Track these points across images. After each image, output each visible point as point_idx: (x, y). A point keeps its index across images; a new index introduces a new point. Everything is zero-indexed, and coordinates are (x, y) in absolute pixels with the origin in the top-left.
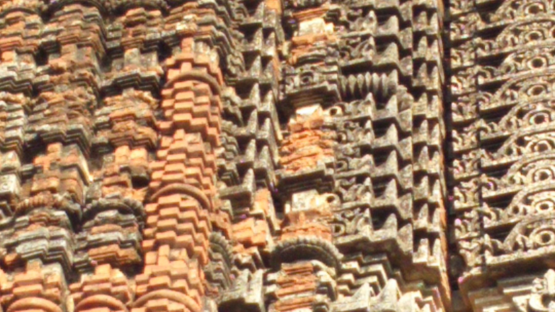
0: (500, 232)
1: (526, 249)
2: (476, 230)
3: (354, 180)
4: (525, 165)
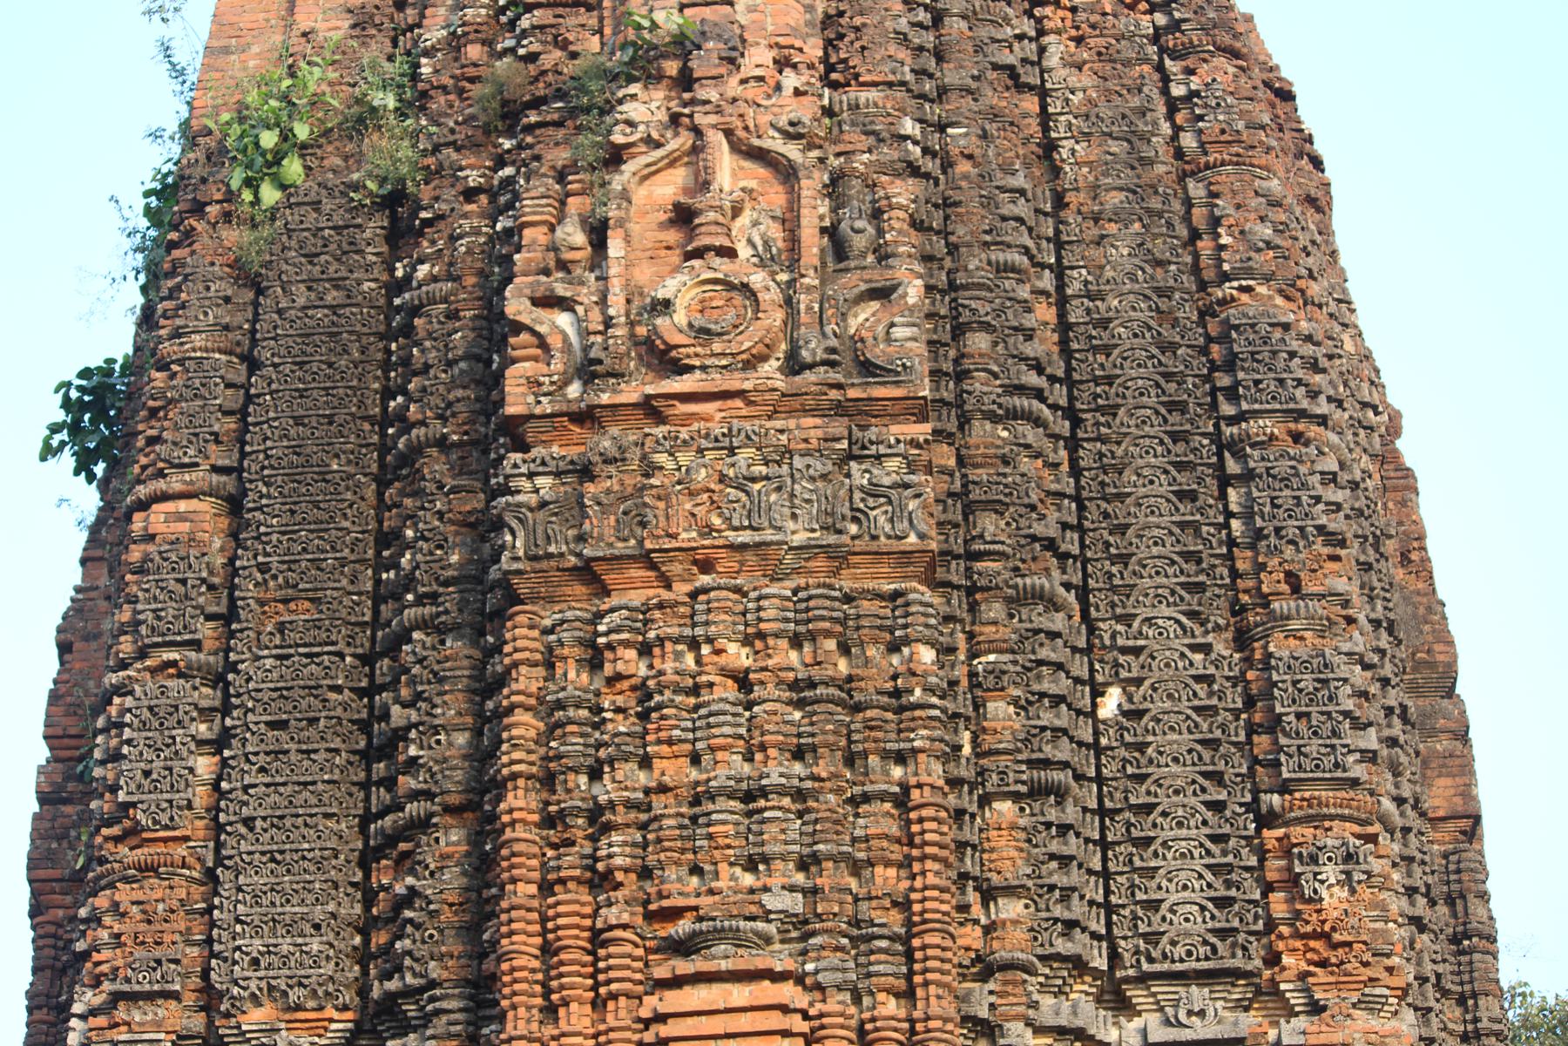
0: (1152, 938)
1: (1173, 961)
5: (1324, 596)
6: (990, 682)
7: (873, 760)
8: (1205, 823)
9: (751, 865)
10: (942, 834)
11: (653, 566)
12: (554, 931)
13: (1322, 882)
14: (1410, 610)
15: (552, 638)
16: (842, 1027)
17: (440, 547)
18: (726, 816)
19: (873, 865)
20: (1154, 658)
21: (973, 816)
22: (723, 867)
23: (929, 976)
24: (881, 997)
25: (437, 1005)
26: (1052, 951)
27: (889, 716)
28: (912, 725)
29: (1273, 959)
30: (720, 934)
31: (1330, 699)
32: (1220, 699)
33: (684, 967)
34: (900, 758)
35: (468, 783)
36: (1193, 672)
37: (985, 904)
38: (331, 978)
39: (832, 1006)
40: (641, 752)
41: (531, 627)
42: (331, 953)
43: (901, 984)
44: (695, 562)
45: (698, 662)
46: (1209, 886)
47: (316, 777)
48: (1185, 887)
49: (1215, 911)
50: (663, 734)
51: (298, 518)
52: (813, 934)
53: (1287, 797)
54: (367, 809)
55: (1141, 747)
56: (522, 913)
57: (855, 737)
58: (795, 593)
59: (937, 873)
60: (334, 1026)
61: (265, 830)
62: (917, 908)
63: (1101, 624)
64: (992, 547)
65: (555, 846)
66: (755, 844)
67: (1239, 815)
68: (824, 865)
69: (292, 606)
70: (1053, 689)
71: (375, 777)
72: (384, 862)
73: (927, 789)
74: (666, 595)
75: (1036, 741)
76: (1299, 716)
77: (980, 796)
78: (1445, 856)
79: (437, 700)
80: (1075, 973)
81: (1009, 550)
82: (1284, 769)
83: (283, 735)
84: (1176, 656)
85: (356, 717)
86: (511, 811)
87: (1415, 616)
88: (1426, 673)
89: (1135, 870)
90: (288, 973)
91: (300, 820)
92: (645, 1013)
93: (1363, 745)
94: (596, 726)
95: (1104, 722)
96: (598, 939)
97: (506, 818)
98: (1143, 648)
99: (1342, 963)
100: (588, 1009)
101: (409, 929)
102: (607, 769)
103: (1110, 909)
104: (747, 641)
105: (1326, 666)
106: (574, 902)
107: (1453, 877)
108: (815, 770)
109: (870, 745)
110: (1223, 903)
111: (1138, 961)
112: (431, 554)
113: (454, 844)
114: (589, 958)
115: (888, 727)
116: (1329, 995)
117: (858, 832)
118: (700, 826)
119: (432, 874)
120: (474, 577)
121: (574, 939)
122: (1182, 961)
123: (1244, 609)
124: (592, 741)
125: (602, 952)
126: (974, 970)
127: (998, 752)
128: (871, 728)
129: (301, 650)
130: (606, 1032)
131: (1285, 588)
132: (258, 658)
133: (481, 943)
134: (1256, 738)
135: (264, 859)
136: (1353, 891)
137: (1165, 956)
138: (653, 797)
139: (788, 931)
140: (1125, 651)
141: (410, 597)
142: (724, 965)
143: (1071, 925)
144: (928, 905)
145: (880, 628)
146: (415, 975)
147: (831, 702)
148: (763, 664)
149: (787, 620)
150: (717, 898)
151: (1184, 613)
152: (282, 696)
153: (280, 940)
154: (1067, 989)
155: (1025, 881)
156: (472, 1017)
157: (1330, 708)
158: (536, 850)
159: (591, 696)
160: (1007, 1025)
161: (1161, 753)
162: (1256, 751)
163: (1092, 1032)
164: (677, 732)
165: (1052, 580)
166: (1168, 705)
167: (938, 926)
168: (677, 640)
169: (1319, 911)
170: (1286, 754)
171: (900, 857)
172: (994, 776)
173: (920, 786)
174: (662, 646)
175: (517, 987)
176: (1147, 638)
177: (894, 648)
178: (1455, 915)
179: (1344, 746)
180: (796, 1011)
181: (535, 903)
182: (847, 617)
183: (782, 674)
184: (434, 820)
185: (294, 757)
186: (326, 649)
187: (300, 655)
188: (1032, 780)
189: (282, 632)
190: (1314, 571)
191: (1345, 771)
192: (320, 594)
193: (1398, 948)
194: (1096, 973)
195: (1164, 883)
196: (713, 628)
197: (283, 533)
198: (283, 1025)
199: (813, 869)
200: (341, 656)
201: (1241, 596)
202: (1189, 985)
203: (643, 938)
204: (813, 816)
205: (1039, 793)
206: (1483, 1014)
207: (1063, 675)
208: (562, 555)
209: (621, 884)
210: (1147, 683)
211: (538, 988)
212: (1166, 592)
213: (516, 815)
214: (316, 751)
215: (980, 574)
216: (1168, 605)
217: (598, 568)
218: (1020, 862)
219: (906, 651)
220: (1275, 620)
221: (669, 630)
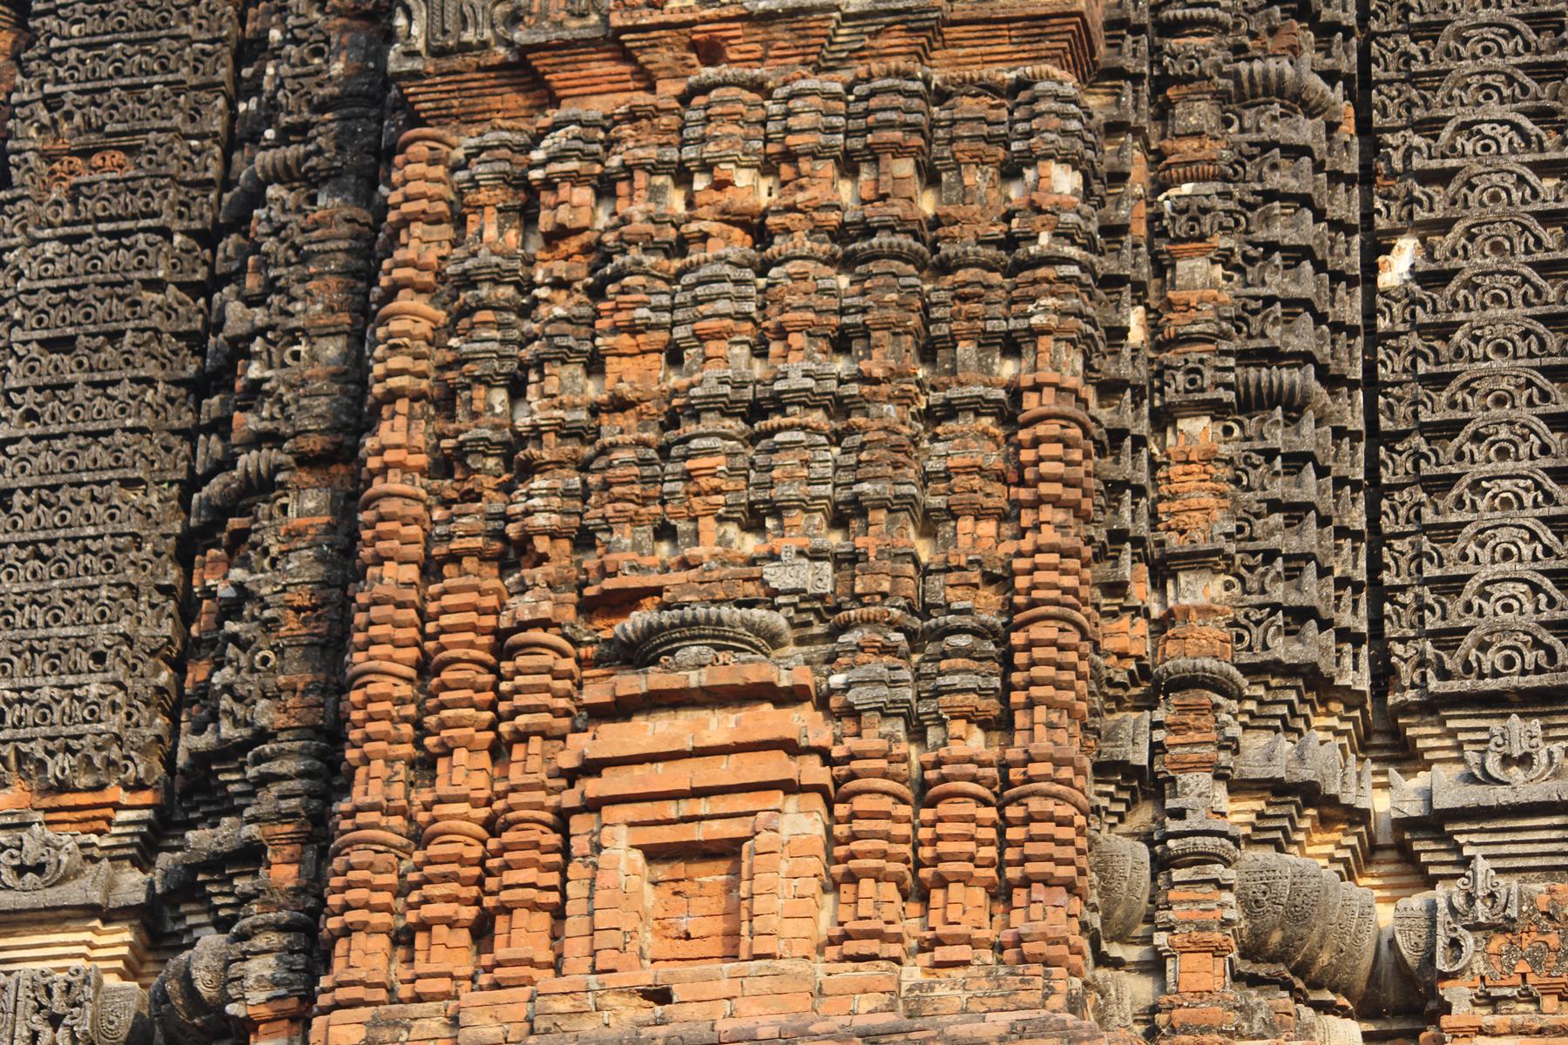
0: (1448, 638)
1: (1482, 676)
2: (1412, 626)
4: (1482, 531)
6: (1181, 227)
7: (966, 349)
8: (1545, 450)
9: (753, 521)
10: (1069, 463)
11: (626, 56)
12: (434, 636)
15: (461, 175)
16: (885, 775)
17: (317, 52)
18: (715, 445)
19: (956, 518)
20: (1472, 187)
21: (1139, 442)
22: (707, 524)
23: (1035, 691)
24: (958, 727)
25: (264, 767)
26: (1267, 656)
27: (996, 278)
28: (1031, 291)
30: (691, 630)
33: (632, 683)
34: (1011, 346)
35: (336, 416)
36: (1537, 206)
37: (1158, 584)
38: (117, 737)
40: (588, 346)
41: (433, 162)
42: (120, 697)
43: (992, 706)
44: (693, 46)
45: (690, 204)
46: (1548, 551)
47: (114, 424)
48: (1507, 555)
49: (1556, 593)
50: (621, 317)
51: (111, 23)
52: (846, 627)
54: (191, 469)
55: (1444, 331)
56: (388, 610)
57: (937, 313)
58: (849, 90)
59: (1060, 527)
60: (123, 816)
61: (28, 509)
62: (1021, 582)
63: (1388, 138)
64: (1195, 12)
65: (446, 503)
66: (758, 486)
69: (96, 160)
70: (1291, 238)
71: (204, 420)
72: (213, 552)
73: (1049, 393)
74: (642, 98)
75: (1255, 322)
77: (1152, 410)
79: (297, 290)
80: (1312, 696)
81: (1227, 18)
83: (67, 361)
84: (1510, 181)
85: (184, 327)
86: (380, 451)
89: (1424, 529)
90: (48, 731)
91: (83, 490)
92: (568, 760)
94: (525, 312)
95: (1385, 294)
96: (503, 646)
97: (374, 463)
98: (1455, 171)
100: (484, 759)
101: (231, 651)
102: (533, 377)
103: (1379, 593)
104: (767, 167)
106: (471, 588)
108: (864, 365)
109: (961, 326)
111: (1424, 677)
112: (304, 63)
113: (309, 514)
114: (488, 678)
115: (992, 296)
117: (933, 465)
118: (674, 460)
119: (273, 562)
120: (367, 96)
121: (466, 648)
122: (1496, 674)
124: (515, 334)
125: (506, 666)
126: (1135, 691)
127: (1190, 339)
128: (965, 299)
129: (103, 227)
130: (503, 795)
132: (35, 242)
133: (221, 625)
135: (23, 554)
138: (604, 417)
139: (809, 624)
140: (1425, 177)
141: (270, 134)
142: (695, 679)
144: (1040, 577)
145: (989, 139)
146: (236, 723)
147: (898, 257)
148: (790, 201)
149: (832, 130)
150: (693, 573)
151: (1527, 113)
152: (68, 300)
153: (39, 681)
154: (1301, 724)
155: (1222, 543)
156: (317, 785)
158: (418, 509)
159: (518, 264)
160: (1183, 778)
161: (1476, 340)
164: (643, 312)
165: (1302, 67)
166: (1492, 261)
167: (1052, 610)
168: (654, 169)
172: (1180, 376)
173: (1037, 388)
174: (631, 179)
175: (371, 727)
176: (1463, 155)
177: (1011, 171)
180: (810, 750)
181: (412, 595)
182: (934, 124)
183: (819, 216)
184: (280, 477)
185: (80, 393)
186: (142, 223)
187: (101, 234)
188: (1246, 384)
189: (74, 201)
192: (139, 140)
194: (1351, 698)
195: (1472, 549)
196: (711, 147)
197: (86, 47)
198: (40, 816)
199: (855, 524)
200: (167, 234)
202: (1506, 716)
203: (576, 644)
204: (858, 439)
205: (1260, 406)
207: (1309, 214)
208: (484, 45)
209: (543, 559)
210: (1458, 228)
211: (407, 729)
213: (390, 456)
214: (115, 383)
215: (1174, 56)
216: (1502, 101)
217: (539, 62)
218: (1217, 514)
219: (1030, 174)
221: (640, 153)
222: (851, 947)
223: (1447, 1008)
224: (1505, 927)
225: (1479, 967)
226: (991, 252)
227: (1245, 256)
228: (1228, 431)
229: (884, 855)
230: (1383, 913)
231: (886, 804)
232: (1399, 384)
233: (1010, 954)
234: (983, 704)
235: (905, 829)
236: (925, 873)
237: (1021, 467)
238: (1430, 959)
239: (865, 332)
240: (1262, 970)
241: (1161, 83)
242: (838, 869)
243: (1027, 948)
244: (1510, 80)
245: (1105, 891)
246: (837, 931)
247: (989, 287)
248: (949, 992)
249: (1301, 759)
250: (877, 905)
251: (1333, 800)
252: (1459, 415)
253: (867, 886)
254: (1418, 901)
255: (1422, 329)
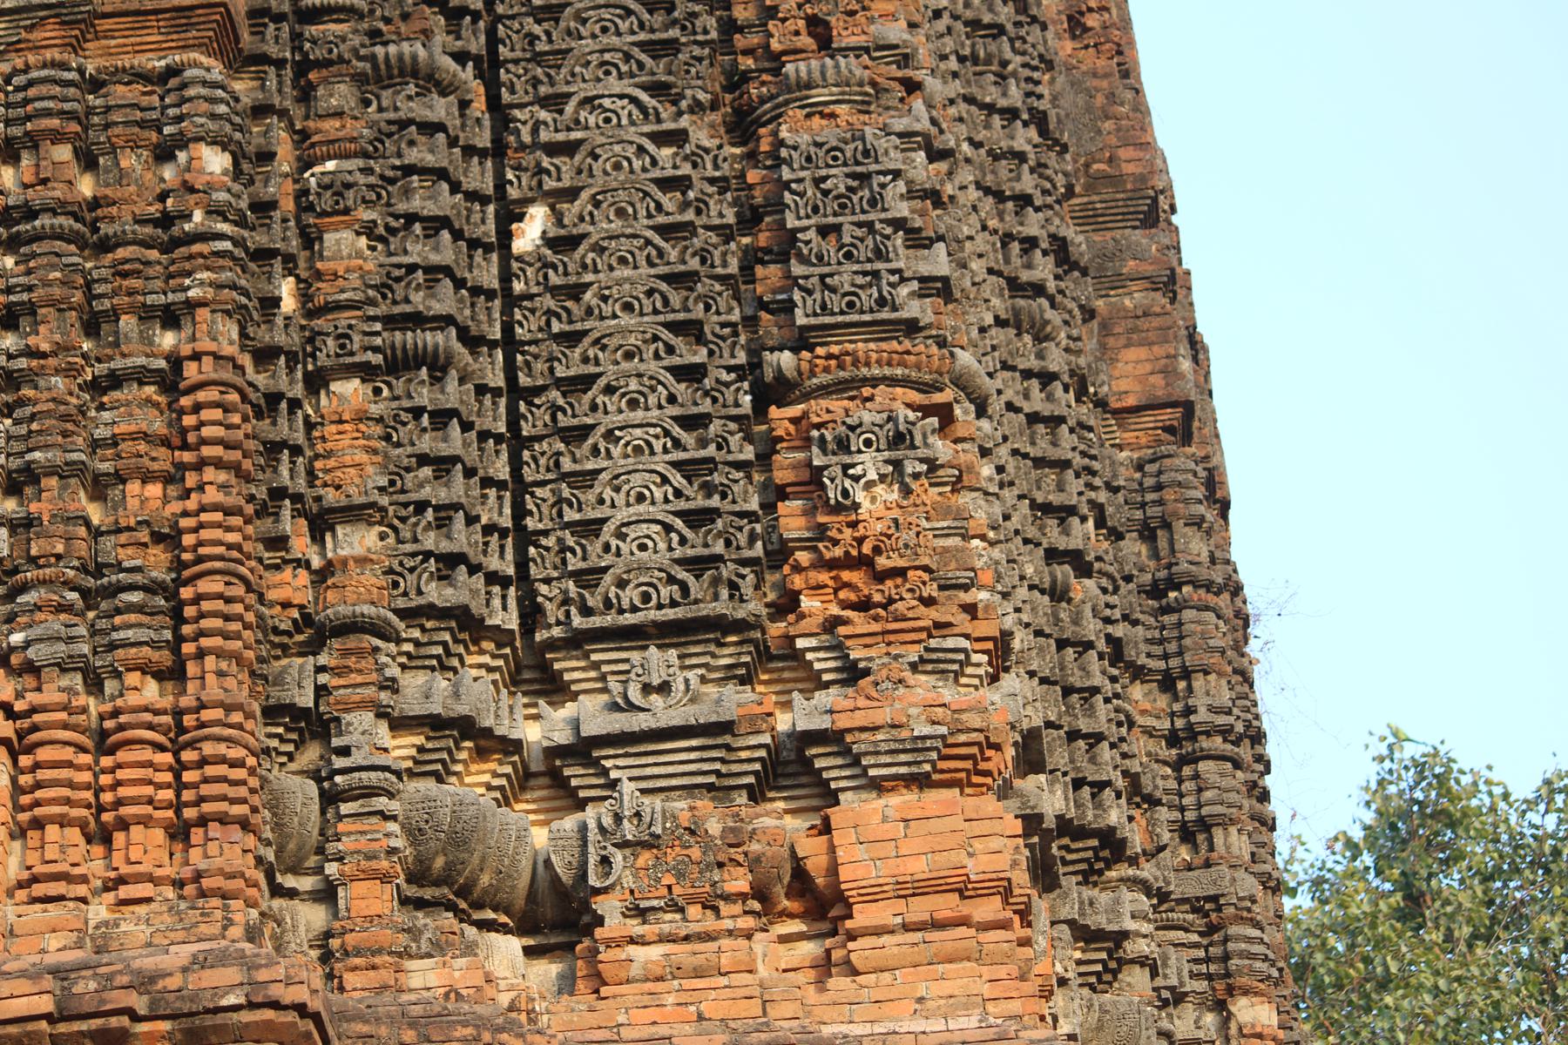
0: (588, 577)
1: (621, 611)
2: (556, 568)
3: (411, 508)
4: (616, 477)
5: (867, 50)
7: (127, 323)
8: (672, 399)
10: (228, 427)
13: (856, 479)
14: (1081, 100)
16: (66, 726)
19: (124, 482)
20: (596, 157)
21: (295, 404)
23: (205, 642)
24: (133, 678)
26: (421, 601)
27: (154, 254)
28: (187, 266)
29: (787, 605)
31: (873, 202)
32: (699, 212)
34: (170, 318)
36: (657, 174)
37: (317, 536)
39: (50, 695)
43: (164, 658)
46: (678, 493)
48: (641, 498)
49: (687, 532)
52: (24, 588)
53: (805, 354)
57: (99, 289)
59: (223, 487)
62: (188, 540)
63: (517, 113)
67: (727, 385)
68: (44, 482)
70: (430, 209)
76: (824, 231)
77: (306, 374)
78: (1140, 467)
80: (465, 636)
82: (798, 312)
84: (631, 151)
87: (1089, 109)
88: (1107, 193)
93: (925, 269)
95: (519, 259)
98: (580, 142)
99: (891, 601)
105: (866, 153)
107: (1150, 497)
108: (32, 341)
110: (698, 518)
111: (568, 614)
115: (151, 272)
116: (872, 653)
117: (101, 433)
123: (745, 77)
126: (300, 638)
127: (339, 307)
128: (125, 275)
131: (806, 41)
134: (760, 271)
136: (907, 491)
137: (608, 604)
140: (553, 149)
143: (451, 561)
144: (205, 534)
145: (142, 124)
147: (60, 237)
154: (455, 662)
155: (375, 497)
157: (871, 217)
160: (347, 717)
161: (605, 299)
162: (759, 290)
163: (487, 722)
165: (434, 48)
166: (617, 225)
167: (218, 565)
169: (853, 525)
170: (802, 288)
171: (168, 466)
172: (330, 342)
173: (196, 356)
176: (587, 128)
177: (164, 154)
178: (1155, 555)
179: (893, 272)
182: (90, 111)
188: (393, 347)
190: (852, 13)
191: (895, 309)
193: (987, 577)
194: (502, 637)
195: (608, 493)
199: (28, 491)
201: (740, 59)
202: (645, 648)
204: (28, 410)
205: (407, 368)
206: (1200, 701)
207: (445, 186)
210: (585, 195)
212: (616, 58)
216: (620, 76)
218: (370, 470)
219: (182, 156)
220: (790, 91)
222: (39, 890)
223: (600, 921)
224: (652, 843)
225: (629, 881)
226: (148, 230)
227: (387, 227)
228: (377, 391)
229: (68, 802)
230: (538, 835)
231: (67, 753)
232: (535, 342)
233: (190, 889)
234: (155, 656)
235: (86, 777)
236: (107, 817)
237: (184, 431)
238: (583, 876)
239: (31, 309)
240: (428, 893)
241: (303, 67)
242: (24, 817)
243: (206, 883)
244: (628, 57)
245: (278, 826)
246: (26, 875)
247: (148, 263)
248: (133, 927)
249: (456, 695)
250: (63, 849)
251: (488, 732)
252: (592, 369)
253: (52, 831)
254: (569, 823)
255: (554, 291)
